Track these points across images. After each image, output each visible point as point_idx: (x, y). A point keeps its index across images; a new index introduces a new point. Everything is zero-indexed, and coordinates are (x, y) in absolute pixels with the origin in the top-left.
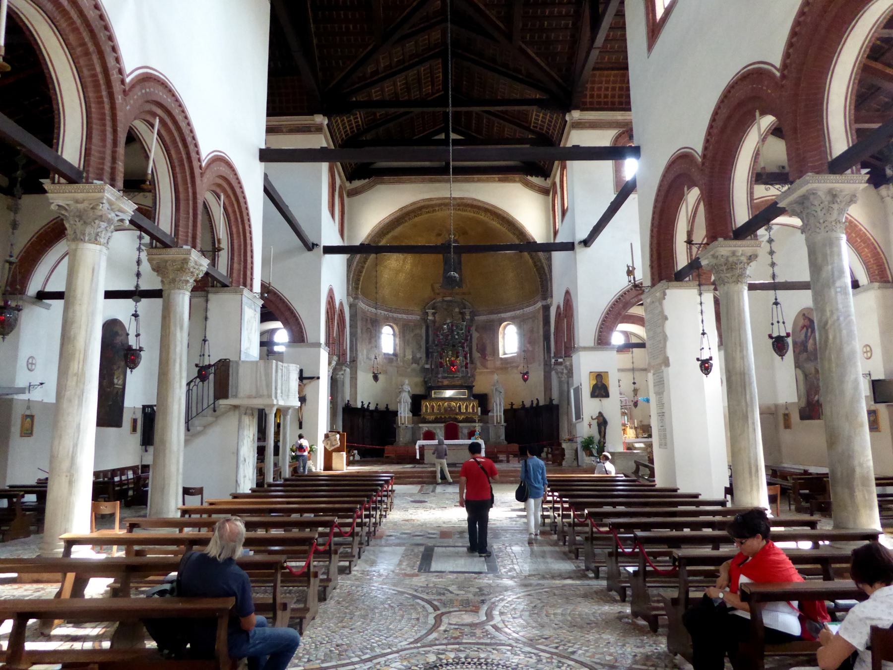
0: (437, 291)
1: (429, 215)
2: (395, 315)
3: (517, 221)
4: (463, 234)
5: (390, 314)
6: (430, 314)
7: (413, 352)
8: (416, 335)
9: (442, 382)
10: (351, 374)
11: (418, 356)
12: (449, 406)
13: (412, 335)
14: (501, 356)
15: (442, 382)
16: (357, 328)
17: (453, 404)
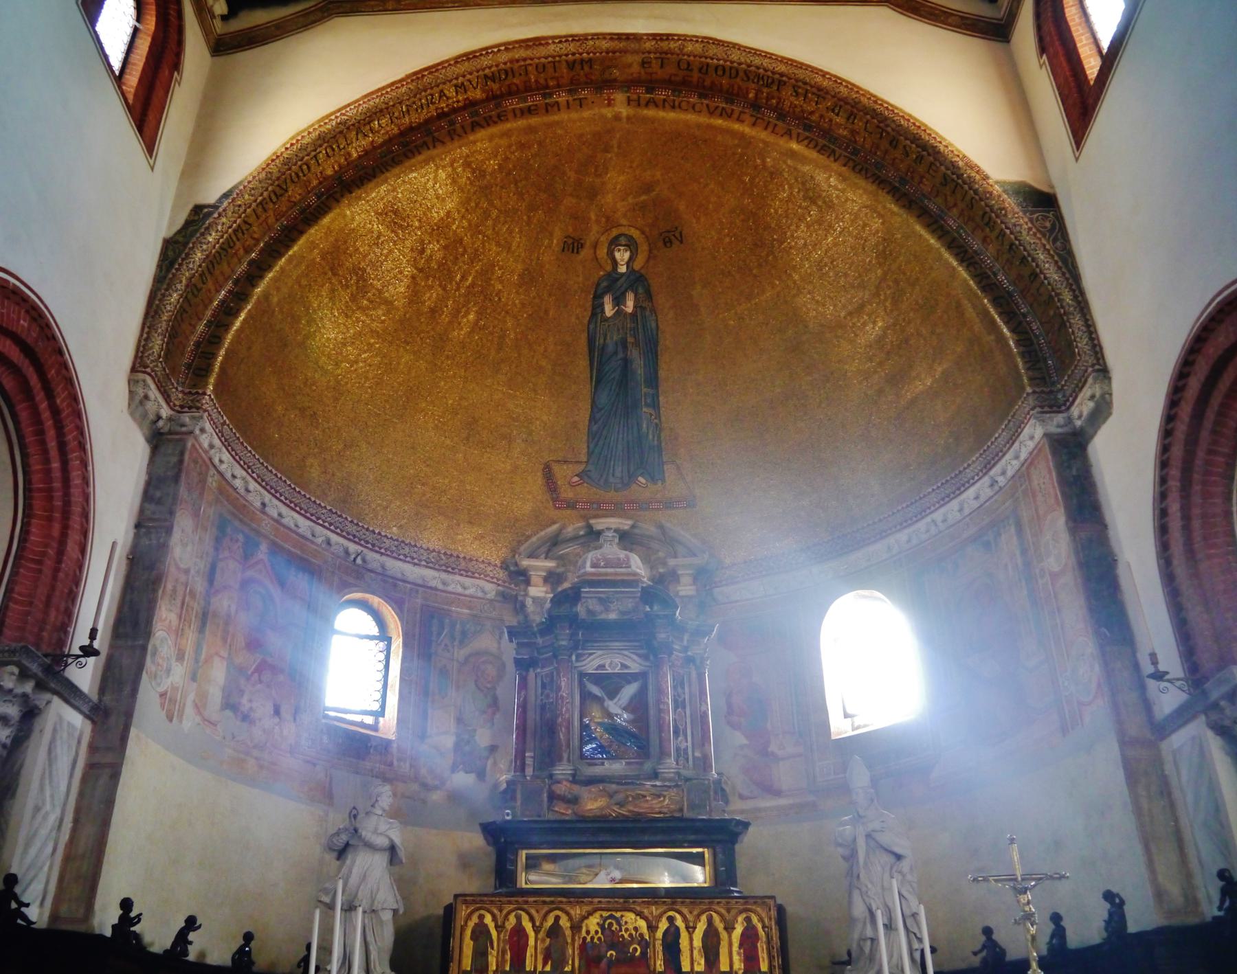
0: (567, 493)
1: (534, 121)
2: (396, 566)
3: (892, 109)
4: (667, 243)
5: (371, 555)
6: (536, 577)
7: (459, 720)
8: (478, 654)
9: (574, 801)
10: (93, 748)
11: (483, 738)
12: (613, 939)
13: (461, 654)
14: (840, 727)
15: (574, 801)
16: (169, 531)
17: (632, 922)
